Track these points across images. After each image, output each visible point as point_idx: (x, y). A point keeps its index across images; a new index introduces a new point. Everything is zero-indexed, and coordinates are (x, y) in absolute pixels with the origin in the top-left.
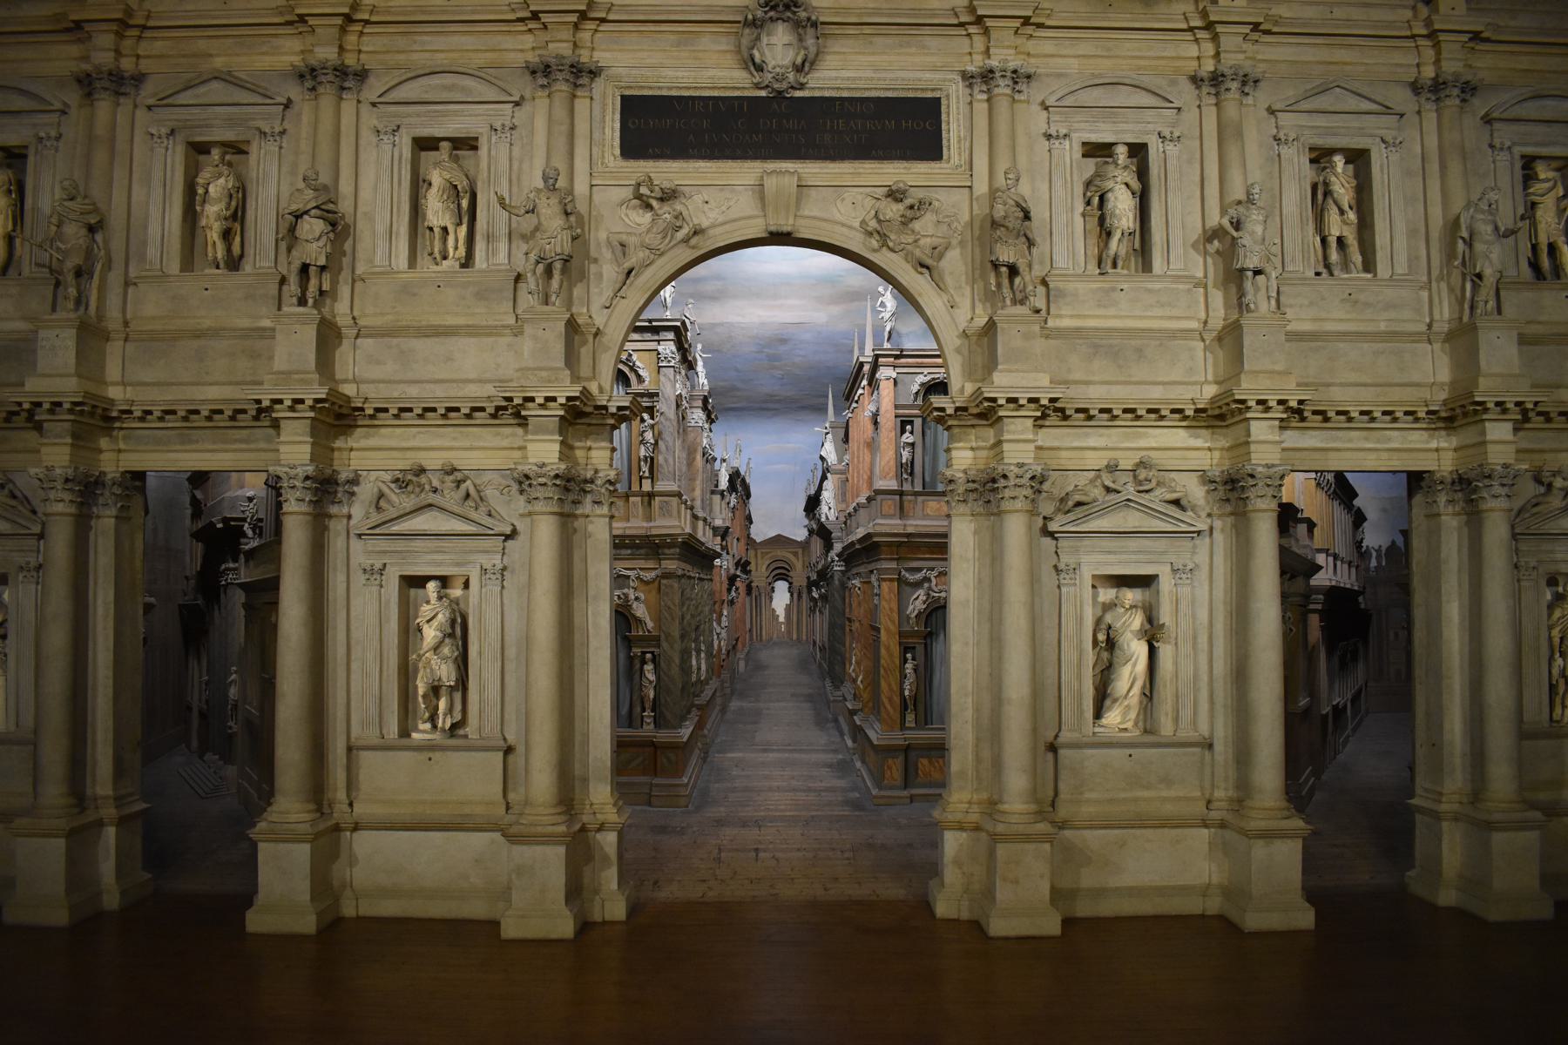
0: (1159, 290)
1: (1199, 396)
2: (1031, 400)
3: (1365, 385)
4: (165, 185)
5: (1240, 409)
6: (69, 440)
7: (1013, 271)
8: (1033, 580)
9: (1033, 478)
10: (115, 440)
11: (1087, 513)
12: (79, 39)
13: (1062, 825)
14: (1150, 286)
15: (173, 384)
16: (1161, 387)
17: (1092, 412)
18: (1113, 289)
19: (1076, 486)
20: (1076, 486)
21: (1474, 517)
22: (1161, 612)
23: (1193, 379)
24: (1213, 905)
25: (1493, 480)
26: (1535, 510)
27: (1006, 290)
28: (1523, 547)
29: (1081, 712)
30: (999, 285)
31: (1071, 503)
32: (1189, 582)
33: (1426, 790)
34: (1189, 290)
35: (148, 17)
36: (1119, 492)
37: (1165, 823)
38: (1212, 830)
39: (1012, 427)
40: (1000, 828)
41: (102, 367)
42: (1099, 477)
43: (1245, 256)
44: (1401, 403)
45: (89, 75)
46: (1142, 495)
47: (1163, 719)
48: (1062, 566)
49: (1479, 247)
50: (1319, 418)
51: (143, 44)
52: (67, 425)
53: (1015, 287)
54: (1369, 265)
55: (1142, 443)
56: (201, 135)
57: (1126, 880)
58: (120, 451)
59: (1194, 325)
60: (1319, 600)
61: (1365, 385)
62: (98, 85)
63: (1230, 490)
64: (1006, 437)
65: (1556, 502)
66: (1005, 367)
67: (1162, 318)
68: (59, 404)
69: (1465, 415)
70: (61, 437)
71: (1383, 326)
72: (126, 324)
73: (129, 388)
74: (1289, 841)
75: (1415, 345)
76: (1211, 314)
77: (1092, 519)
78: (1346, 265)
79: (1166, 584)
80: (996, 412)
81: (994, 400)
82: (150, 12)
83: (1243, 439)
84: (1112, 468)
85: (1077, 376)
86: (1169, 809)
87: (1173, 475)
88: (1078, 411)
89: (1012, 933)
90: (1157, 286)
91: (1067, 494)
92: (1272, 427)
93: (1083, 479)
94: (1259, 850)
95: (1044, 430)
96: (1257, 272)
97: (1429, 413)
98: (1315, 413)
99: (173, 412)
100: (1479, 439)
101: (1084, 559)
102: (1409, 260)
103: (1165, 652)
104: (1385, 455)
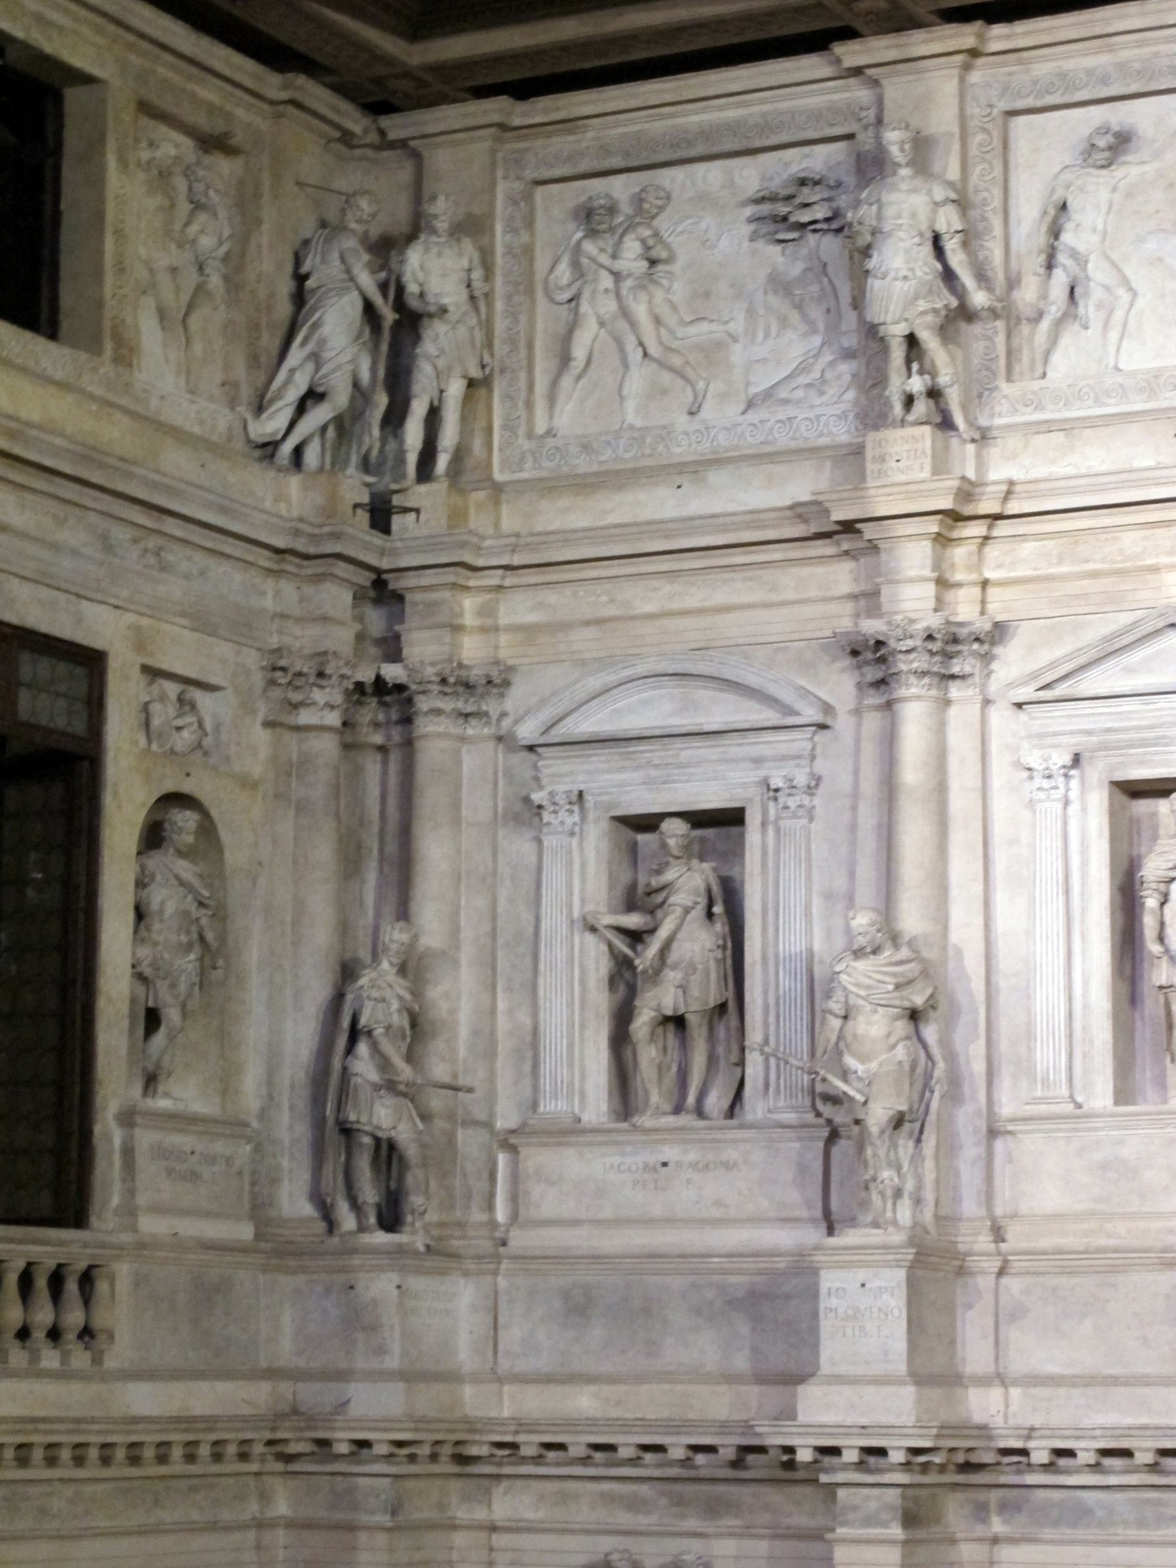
4: (1067, 892)
6: (896, 1531)
10: (981, 1512)
12: (846, 553)
15: (1113, 1381)
35: (1008, 496)
41: (950, 1341)
45: (880, 644)
51: (993, 552)
52: (893, 1495)
56: (1143, 763)
58: (995, 1540)
62: (903, 664)
68: (881, 1452)
70: (885, 1525)
72: (998, 1234)
73: (1015, 1392)
82: (1011, 483)
99: (1127, 1453)
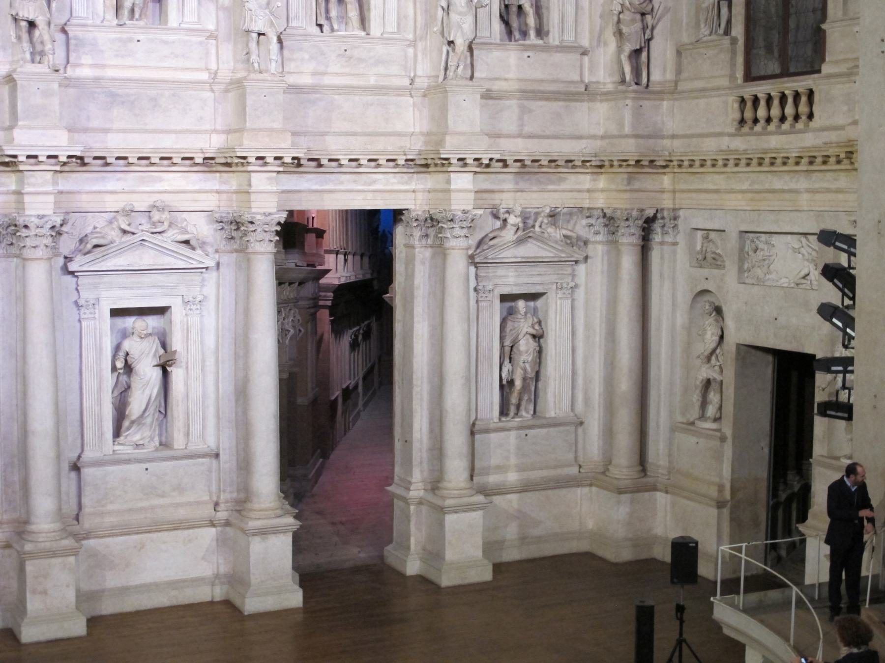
0: (173, 42)
1: (207, 146)
2: (49, 157)
3: (354, 134)
5: (242, 163)
7: (32, 25)
8: (54, 317)
9: (53, 227)
11: (105, 253)
13: (87, 536)
14: (164, 37)
16: (173, 135)
17: (109, 160)
18: (130, 40)
19: (95, 228)
20: (95, 228)
21: (440, 250)
22: (174, 339)
23: (203, 128)
24: (218, 593)
25: (455, 223)
26: (492, 243)
27: (26, 45)
28: (482, 273)
29: (101, 435)
30: (19, 38)
31: (89, 246)
32: (198, 312)
33: (401, 479)
34: (201, 43)
36: (133, 234)
37: (178, 526)
38: (219, 529)
39: (32, 180)
40: (28, 547)
42: (115, 218)
43: (251, 20)
44: (383, 152)
46: (155, 236)
47: (176, 435)
48: (82, 302)
49: (453, 15)
50: (314, 164)
53: (35, 40)
54: (363, 22)
55: (158, 187)
57: (147, 577)
59: (205, 76)
60: (328, 299)
61: (354, 134)
63: (235, 230)
64: (27, 189)
65: (509, 235)
66: (26, 123)
67: (176, 69)
69: (436, 165)
71: (372, 81)
74: (281, 536)
75: (399, 98)
76: (221, 66)
77: (110, 258)
78: (344, 18)
79: (177, 314)
80: (17, 166)
81: (15, 156)
83: (246, 188)
84: (129, 212)
85: (95, 123)
86: (181, 513)
87: (185, 215)
88: (96, 158)
89: (43, 638)
90: (172, 38)
91: (86, 236)
92: (270, 179)
93: (100, 221)
94: (257, 546)
95: (65, 174)
96: (260, 34)
97: (407, 160)
98: (310, 160)
100: (445, 186)
101: (104, 294)
102: (399, 18)
103: (177, 374)
104: (370, 196)
